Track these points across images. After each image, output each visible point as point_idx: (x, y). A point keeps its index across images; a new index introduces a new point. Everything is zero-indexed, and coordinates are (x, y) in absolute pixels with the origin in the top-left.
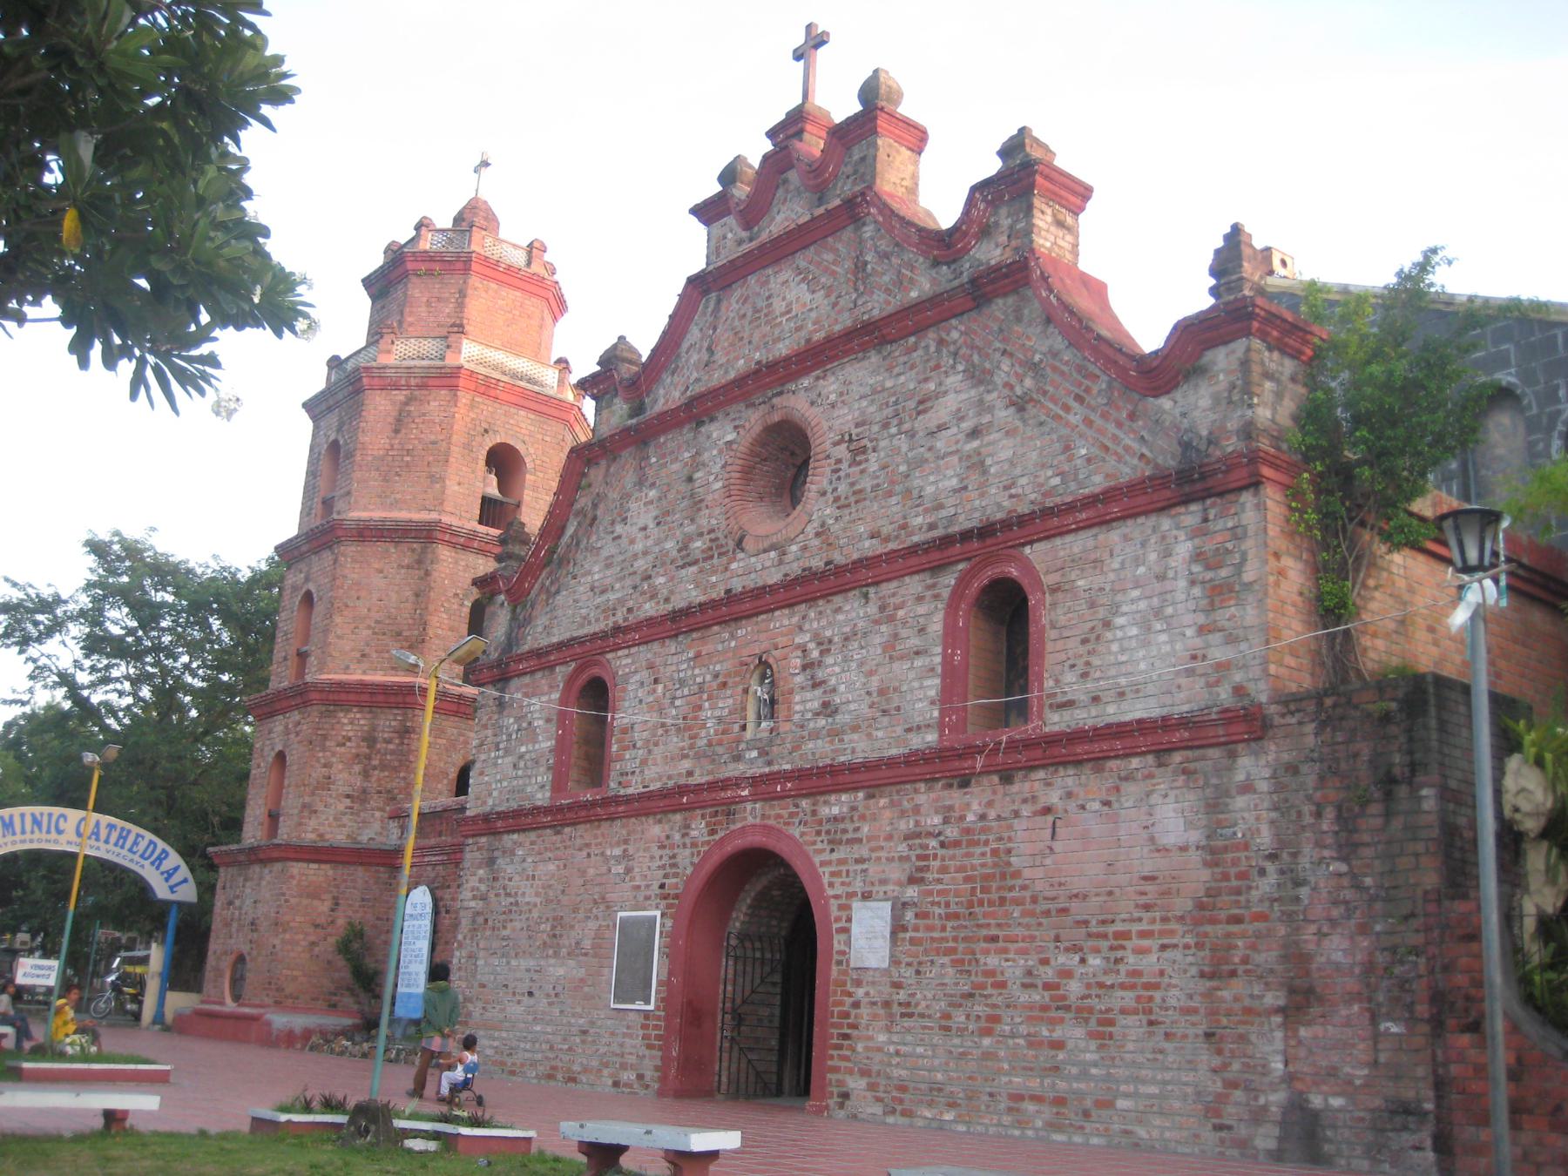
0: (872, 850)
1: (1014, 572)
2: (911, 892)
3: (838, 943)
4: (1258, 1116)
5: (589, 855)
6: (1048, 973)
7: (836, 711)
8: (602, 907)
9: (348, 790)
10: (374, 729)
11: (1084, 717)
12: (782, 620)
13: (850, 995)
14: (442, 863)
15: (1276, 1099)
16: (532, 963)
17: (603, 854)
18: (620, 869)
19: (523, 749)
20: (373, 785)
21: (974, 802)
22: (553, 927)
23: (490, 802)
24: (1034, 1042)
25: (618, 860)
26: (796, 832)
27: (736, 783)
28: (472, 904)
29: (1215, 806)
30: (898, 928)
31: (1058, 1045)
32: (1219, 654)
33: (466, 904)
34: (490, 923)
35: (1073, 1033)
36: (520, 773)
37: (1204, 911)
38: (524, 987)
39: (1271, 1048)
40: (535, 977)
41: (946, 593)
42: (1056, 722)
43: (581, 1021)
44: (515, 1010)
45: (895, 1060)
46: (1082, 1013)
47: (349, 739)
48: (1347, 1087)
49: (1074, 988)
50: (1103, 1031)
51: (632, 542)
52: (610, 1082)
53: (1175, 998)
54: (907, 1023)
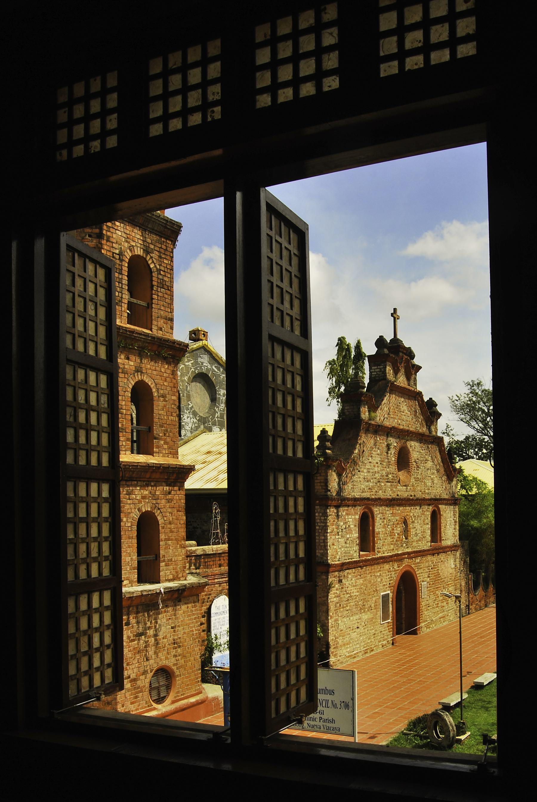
0: (423, 570)
2: (428, 579)
5: (371, 576)
8: (376, 592)
13: (422, 605)
16: (357, 617)
17: (375, 575)
19: (348, 536)
22: (363, 602)
28: (335, 599)
31: (444, 607)
33: (332, 600)
34: (342, 606)
36: (348, 545)
38: (356, 626)
40: (359, 621)
43: (373, 631)
44: (354, 635)
45: (428, 617)
51: (374, 466)
52: (381, 646)
54: (429, 608)
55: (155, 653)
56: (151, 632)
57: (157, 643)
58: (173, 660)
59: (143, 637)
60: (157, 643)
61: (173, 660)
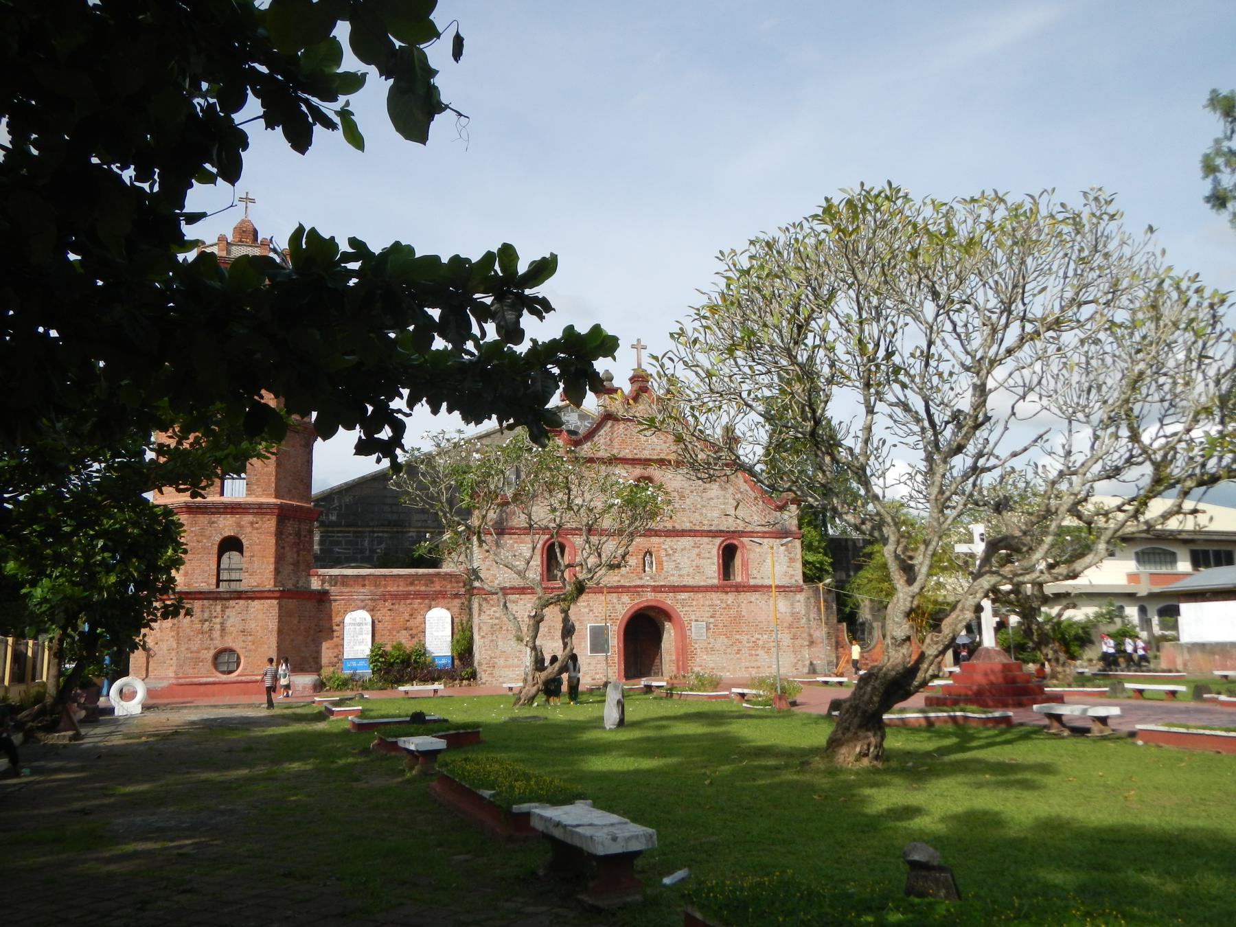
1: (736, 542)
3: (688, 633)
4: (804, 666)
6: (754, 639)
7: (680, 569)
9: (291, 560)
10: (300, 529)
11: (759, 582)
12: (655, 540)
14: (371, 600)
15: (807, 663)
18: (587, 610)
20: (301, 558)
21: (730, 598)
23: (497, 582)
24: (751, 655)
25: (585, 607)
26: (669, 602)
27: (647, 586)
29: (792, 605)
30: (708, 629)
32: (791, 571)
34: (504, 628)
35: (760, 652)
37: (790, 627)
39: (806, 653)
41: (718, 544)
42: (752, 582)
46: (763, 648)
47: (290, 534)
48: (821, 659)
49: (760, 643)
50: (768, 651)
53: (785, 644)
55: (222, 636)
56: (218, 620)
57: (223, 630)
58: (242, 644)
59: (207, 623)
60: (223, 630)
61: (242, 644)
